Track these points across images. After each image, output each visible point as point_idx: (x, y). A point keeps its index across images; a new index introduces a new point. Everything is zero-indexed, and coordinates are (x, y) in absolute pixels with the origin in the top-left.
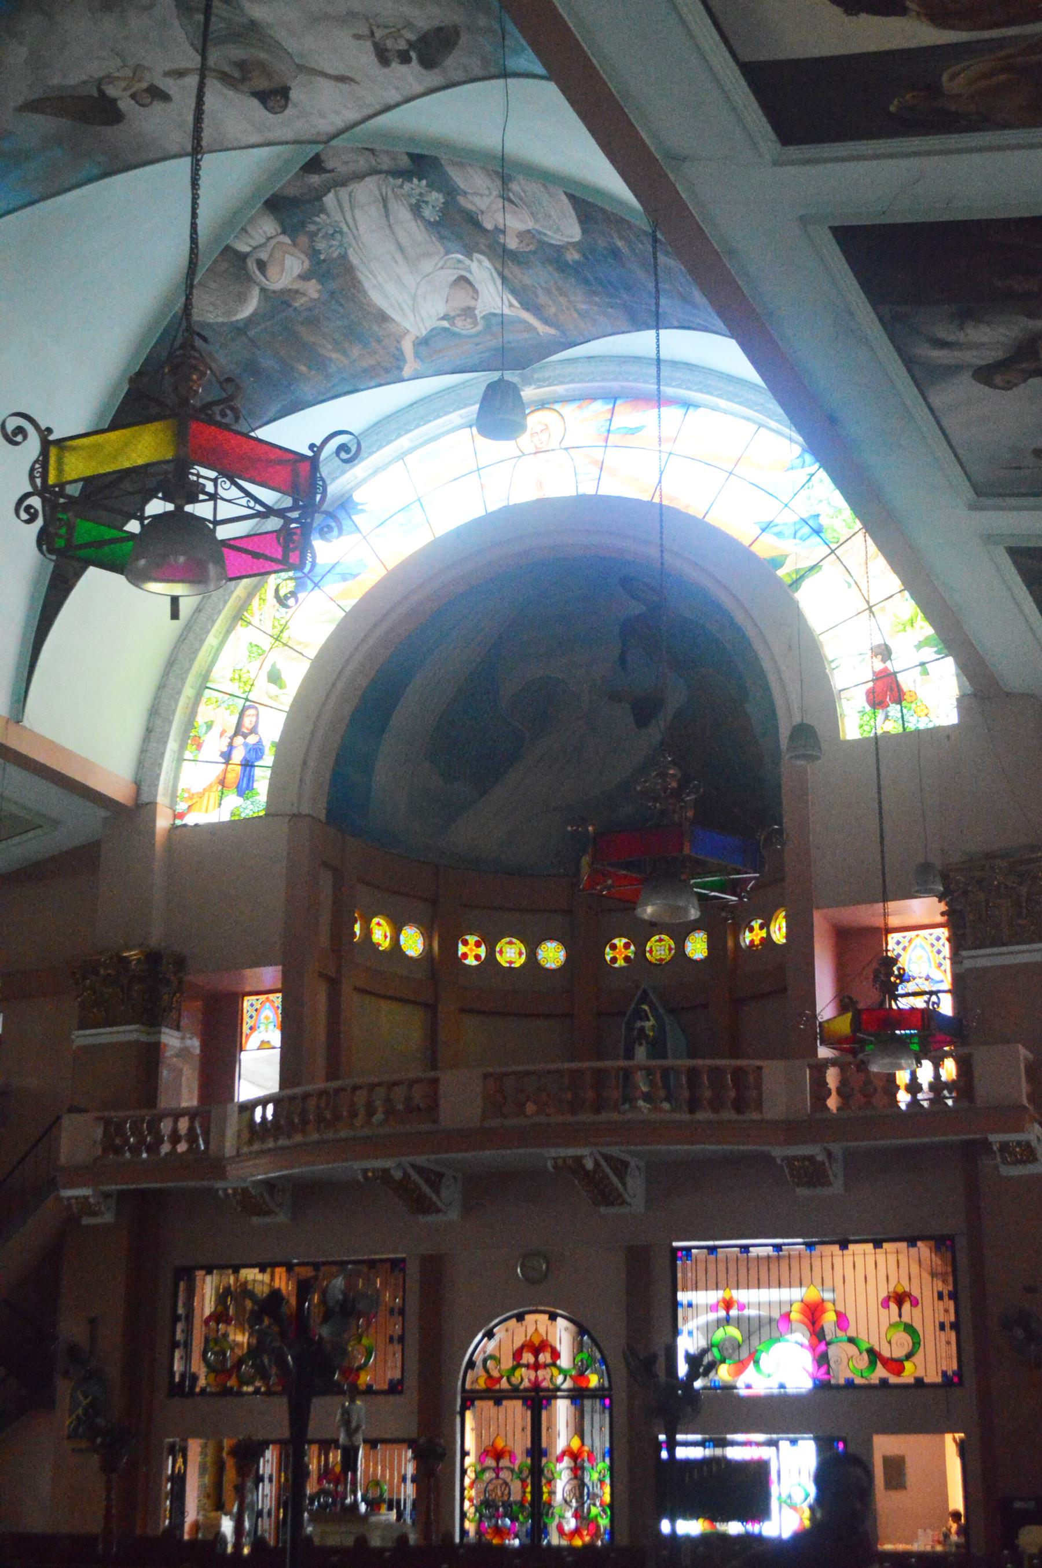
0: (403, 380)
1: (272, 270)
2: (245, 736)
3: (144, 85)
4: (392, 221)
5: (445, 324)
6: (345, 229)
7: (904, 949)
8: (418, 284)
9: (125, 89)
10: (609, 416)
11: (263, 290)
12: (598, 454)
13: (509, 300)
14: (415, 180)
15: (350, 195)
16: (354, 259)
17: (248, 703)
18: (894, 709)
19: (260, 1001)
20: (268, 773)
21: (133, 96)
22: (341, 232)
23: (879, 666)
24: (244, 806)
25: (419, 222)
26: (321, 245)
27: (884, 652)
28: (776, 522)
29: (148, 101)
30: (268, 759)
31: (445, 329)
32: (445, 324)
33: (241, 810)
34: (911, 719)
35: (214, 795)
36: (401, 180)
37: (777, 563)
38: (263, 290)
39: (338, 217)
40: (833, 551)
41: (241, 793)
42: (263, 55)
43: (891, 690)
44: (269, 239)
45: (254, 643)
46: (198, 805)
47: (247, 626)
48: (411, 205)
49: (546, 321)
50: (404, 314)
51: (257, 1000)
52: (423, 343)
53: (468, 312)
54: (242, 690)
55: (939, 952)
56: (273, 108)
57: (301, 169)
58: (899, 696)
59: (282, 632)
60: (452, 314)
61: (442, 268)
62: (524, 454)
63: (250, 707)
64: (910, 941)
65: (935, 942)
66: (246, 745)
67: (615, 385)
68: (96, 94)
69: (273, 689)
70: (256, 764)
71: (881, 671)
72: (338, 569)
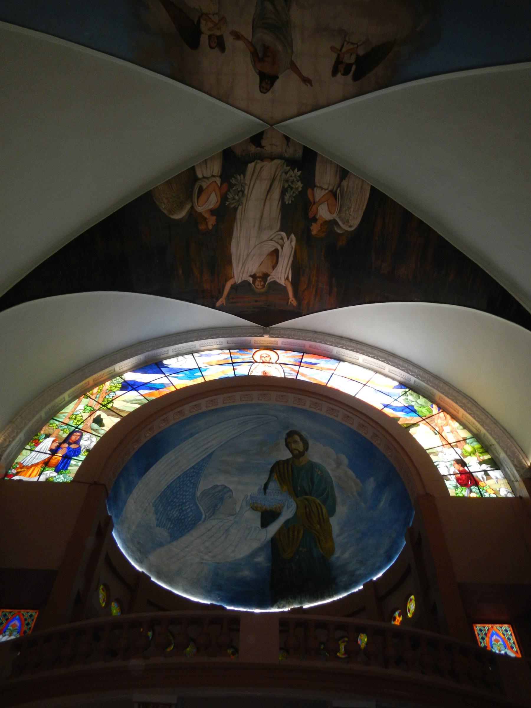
0: (214, 307)
1: (203, 197)
2: (70, 444)
3: (218, 33)
4: (268, 198)
5: (251, 280)
6: (246, 192)
7: (486, 634)
8: (255, 246)
9: (210, 29)
10: (301, 358)
11: (192, 207)
12: (297, 368)
13: (288, 273)
14: (296, 170)
15: (261, 168)
16: (238, 216)
17: (77, 430)
18: (474, 489)
19: (12, 614)
20: (80, 464)
21: (210, 37)
22: (243, 192)
23: (461, 469)
24: (57, 477)
25: (280, 202)
26: (230, 196)
27: (461, 462)
28: (392, 404)
29: (214, 45)
30: (82, 457)
31: (249, 283)
32: (251, 280)
33: (55, 479)
34: (485, 494)
35: (38, 469)
36: (290, 167)
37: (395, 420)
38: (192, 207)
39: (247, 182)
40: (424, 420)
41: (57, 470)
42: (279, 47)
43: (471, 480)
44: (213, 176)
45: (89, 405)
46: (25, 472)
47: (87, 398)
48: (283, 187)
49: (295, 295)
50: (238, 263)
51: (10, 612)
52: (235, 288)
53: (265, 276)
54: (75, 423)
55: (509, 639)
56: (263, 88)
57: (251, 138)
58: (476, 483)
59: (108, 403)
60: (258, 275)
61: (271, 240)
62: (256, 362)
63: (77, 432)
64: (488, 630)
65: (505, 633)
66: (68, 448)
67: (307, 344)
68: (196, 21)
69: (96, 426)
70: (73, 458)
71: (462, 471)
72: (148, 385)
